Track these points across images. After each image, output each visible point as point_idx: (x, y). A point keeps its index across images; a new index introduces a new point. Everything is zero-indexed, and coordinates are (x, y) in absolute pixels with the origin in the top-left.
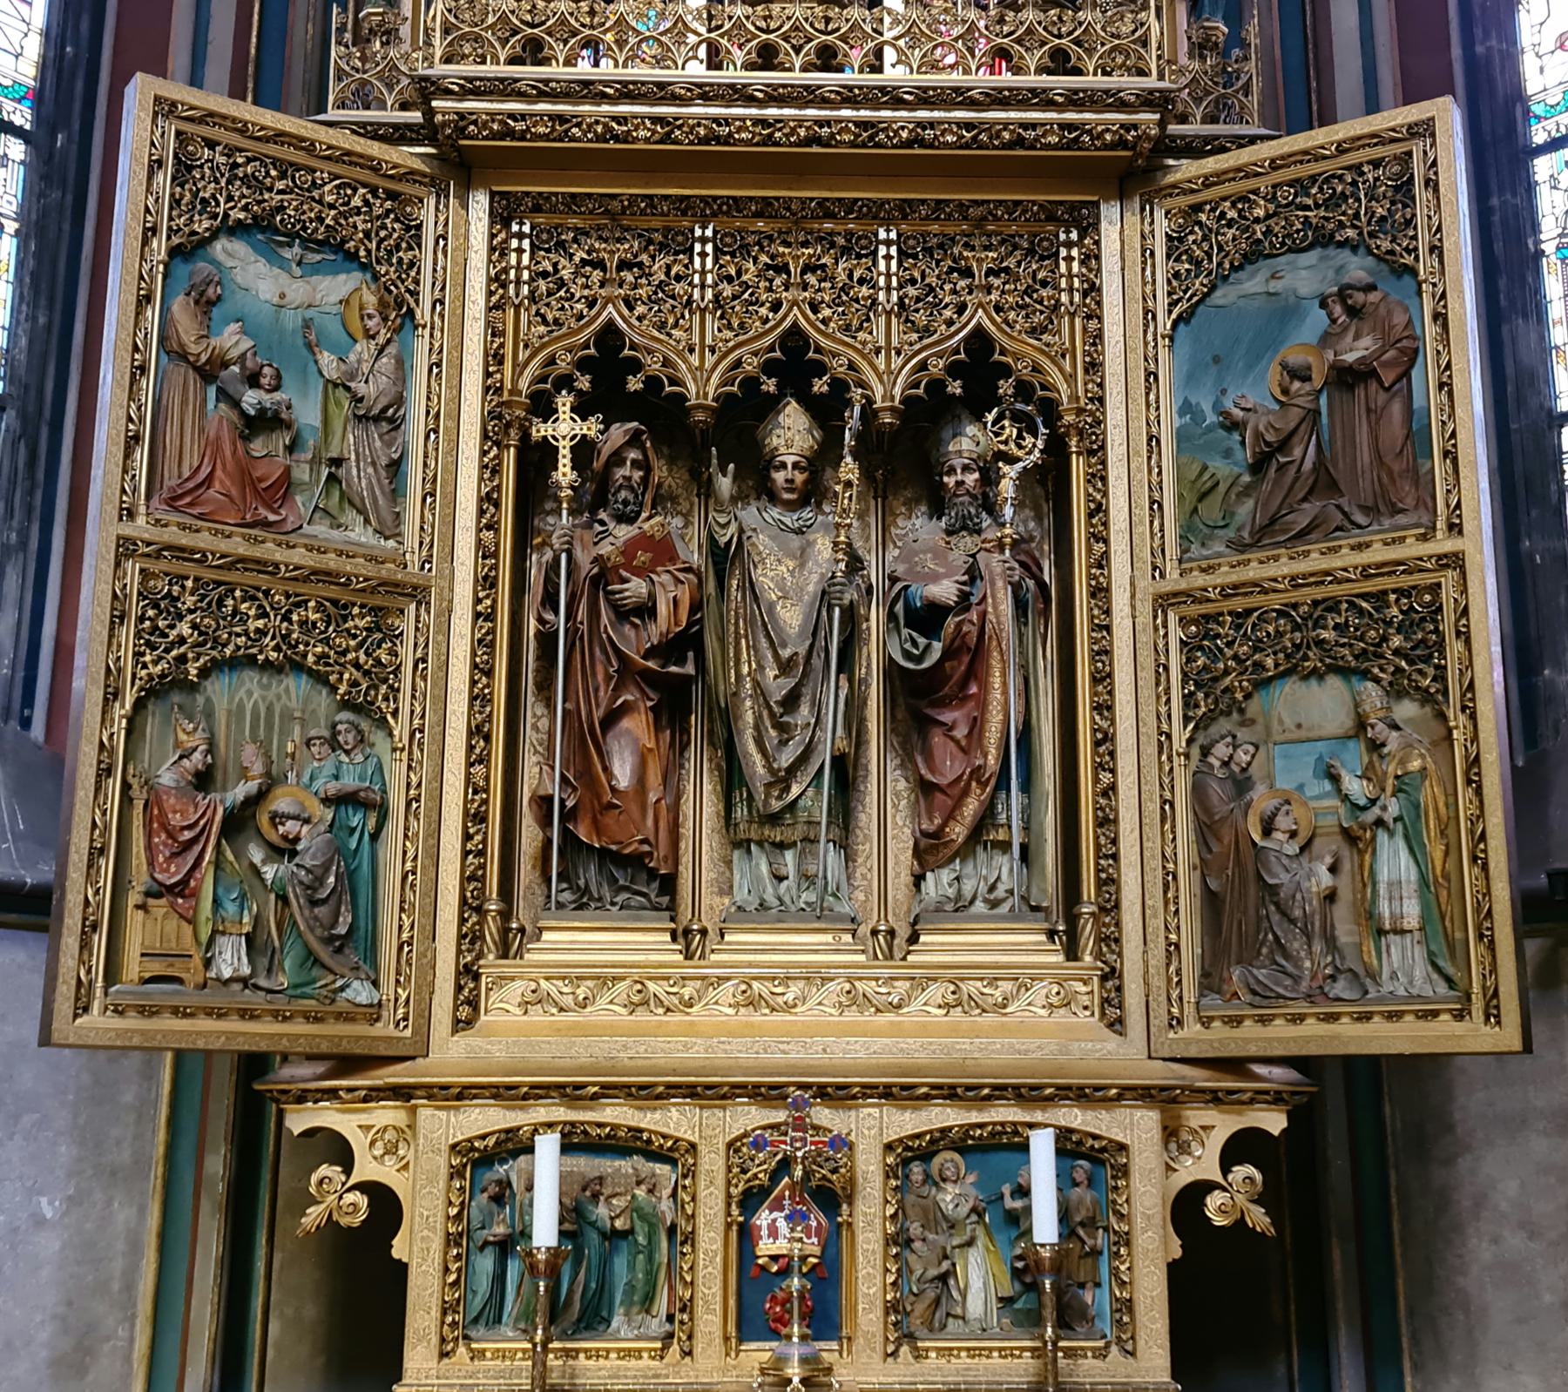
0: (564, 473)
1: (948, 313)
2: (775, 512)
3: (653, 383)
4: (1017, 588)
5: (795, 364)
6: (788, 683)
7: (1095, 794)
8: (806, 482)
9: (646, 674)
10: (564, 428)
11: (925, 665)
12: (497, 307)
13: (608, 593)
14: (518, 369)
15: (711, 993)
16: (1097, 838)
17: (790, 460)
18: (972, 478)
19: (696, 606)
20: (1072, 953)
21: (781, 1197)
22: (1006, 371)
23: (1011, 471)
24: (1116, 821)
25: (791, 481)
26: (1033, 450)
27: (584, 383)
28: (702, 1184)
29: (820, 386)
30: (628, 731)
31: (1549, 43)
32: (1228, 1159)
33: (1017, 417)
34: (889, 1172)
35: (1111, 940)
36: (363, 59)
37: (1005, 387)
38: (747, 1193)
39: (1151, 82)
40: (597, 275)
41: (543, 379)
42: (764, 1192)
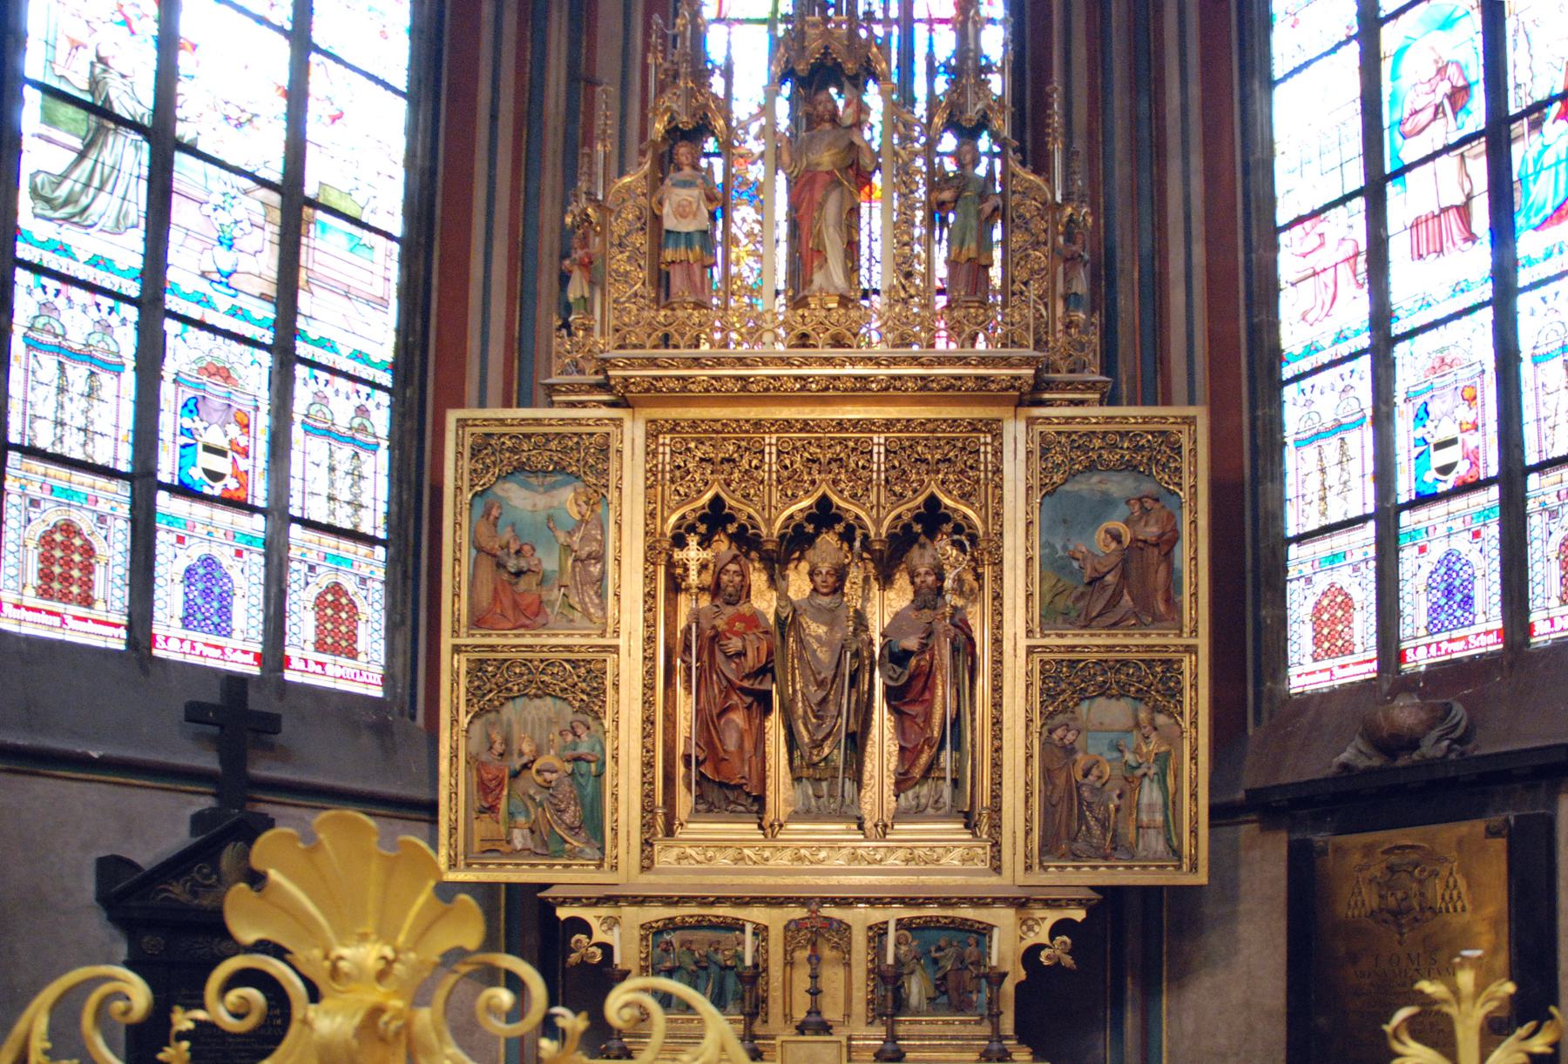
3: (742, 528)
6: (821, 694)
10: (692, 554)
14: (664, 520)
18: (930, 579)
19: (770, 653)
22: (947, 519)
27: (702, 528)
34: (870, 939)
35: (996, 826)
39: (1030, 352)
41: (679, 527)
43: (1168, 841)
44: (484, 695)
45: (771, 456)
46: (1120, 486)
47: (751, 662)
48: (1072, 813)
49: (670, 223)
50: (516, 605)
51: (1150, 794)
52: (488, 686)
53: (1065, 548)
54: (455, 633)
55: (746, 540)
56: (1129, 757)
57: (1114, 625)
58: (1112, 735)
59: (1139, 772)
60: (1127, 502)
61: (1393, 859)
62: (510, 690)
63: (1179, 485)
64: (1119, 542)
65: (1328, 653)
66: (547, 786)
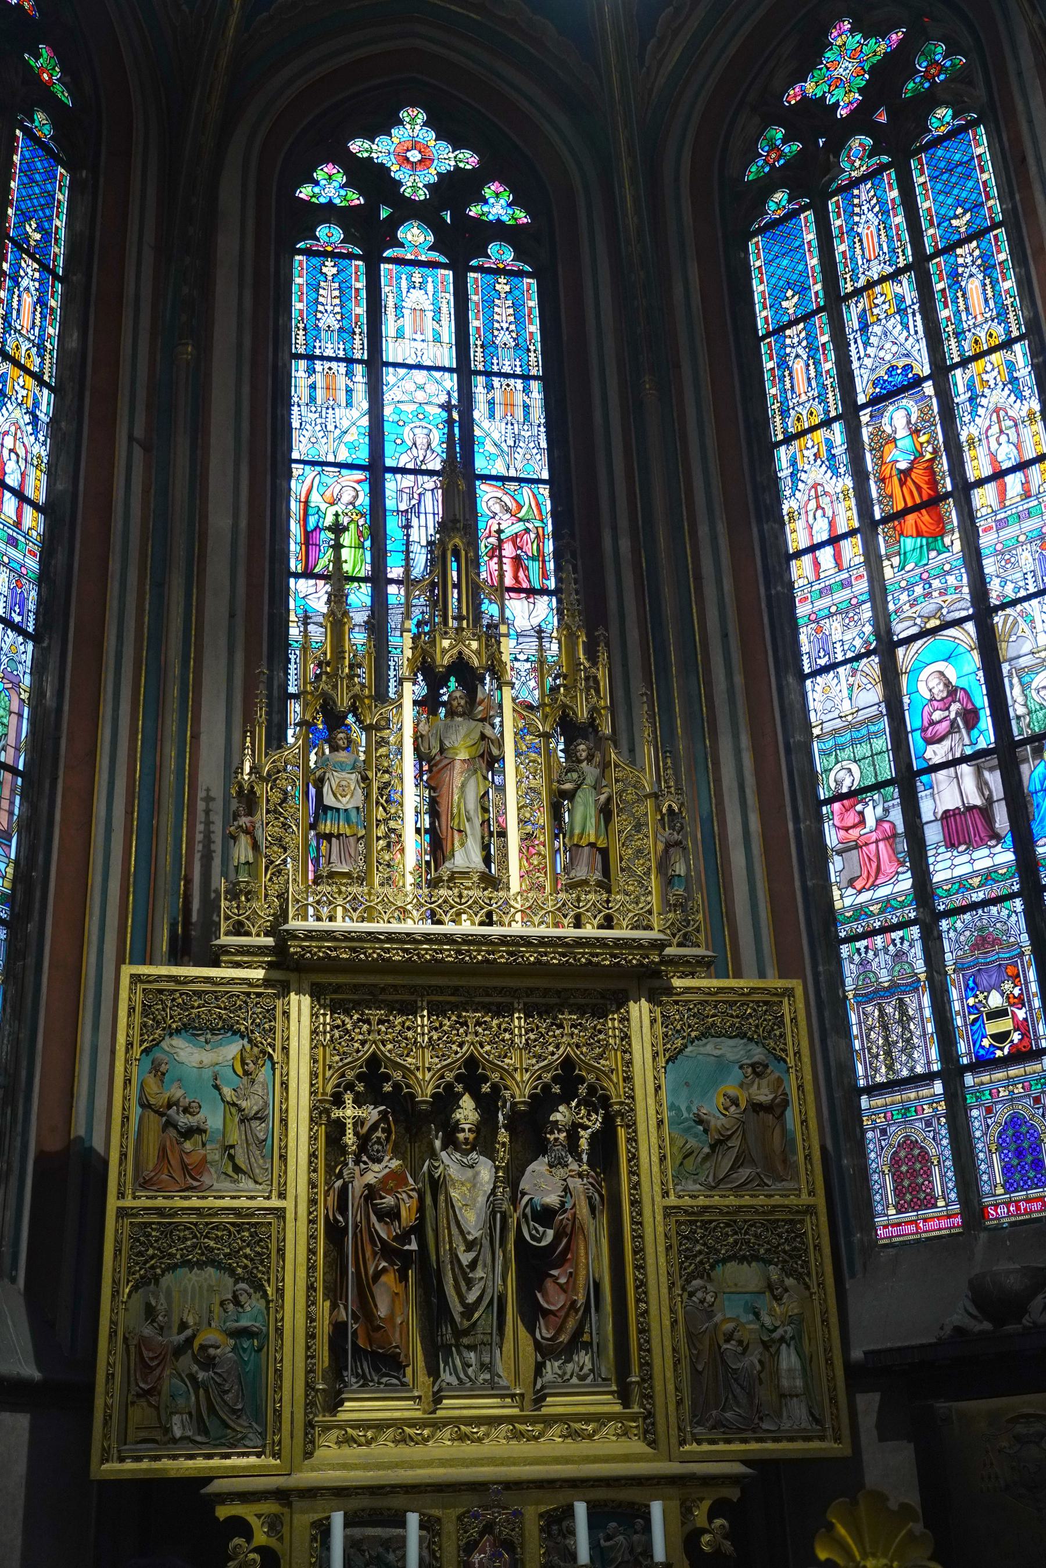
0: (350, 1138)
1: (551, 1048)
2: (458, 1155)
3: (397, 1086)
4: (590, 1198)
5: (472, 1074)
6: (471, 1255)
7: (637, 1316)
8: (475, 1139)
10: (349, 1112)
11: (543, 1244)
12: (316, 1047)
13: (374, 1205)
15: (439, 1434)
16: (639, 1339)
17: (467, 1127)
20: (626, 1405)
21: (485, 1545)
23: (585, 1134)
24: (649, 1331)
25: (466, 1139)
26: (596, 1121)
28: (444, 1540)
29: (486, 1088)
30: (385, 1284)
31: (844, 884)
32: (712, 1516)
34: (542, 1530)
36: (238, 908)
37: (582, 1090)
38: (467, 1544)
40: (365, 1027)
41: (338, 1086)
42: (476, 1543)
44: (146, 1262)
46: (731, 1049)
48: (721, 1387)
49: (329, 800)
50: (184, 1166)
52: (150, 1252)
54: (121, 1195)
56: (767, 1320)
58: (747, 1297)
59: (776, 1335)
60: (741, 1067)
61: (1020, 1429)
62: (172, 1256)
63: (784, 1050)
64: (737, 1105)
65: (915, 1205)
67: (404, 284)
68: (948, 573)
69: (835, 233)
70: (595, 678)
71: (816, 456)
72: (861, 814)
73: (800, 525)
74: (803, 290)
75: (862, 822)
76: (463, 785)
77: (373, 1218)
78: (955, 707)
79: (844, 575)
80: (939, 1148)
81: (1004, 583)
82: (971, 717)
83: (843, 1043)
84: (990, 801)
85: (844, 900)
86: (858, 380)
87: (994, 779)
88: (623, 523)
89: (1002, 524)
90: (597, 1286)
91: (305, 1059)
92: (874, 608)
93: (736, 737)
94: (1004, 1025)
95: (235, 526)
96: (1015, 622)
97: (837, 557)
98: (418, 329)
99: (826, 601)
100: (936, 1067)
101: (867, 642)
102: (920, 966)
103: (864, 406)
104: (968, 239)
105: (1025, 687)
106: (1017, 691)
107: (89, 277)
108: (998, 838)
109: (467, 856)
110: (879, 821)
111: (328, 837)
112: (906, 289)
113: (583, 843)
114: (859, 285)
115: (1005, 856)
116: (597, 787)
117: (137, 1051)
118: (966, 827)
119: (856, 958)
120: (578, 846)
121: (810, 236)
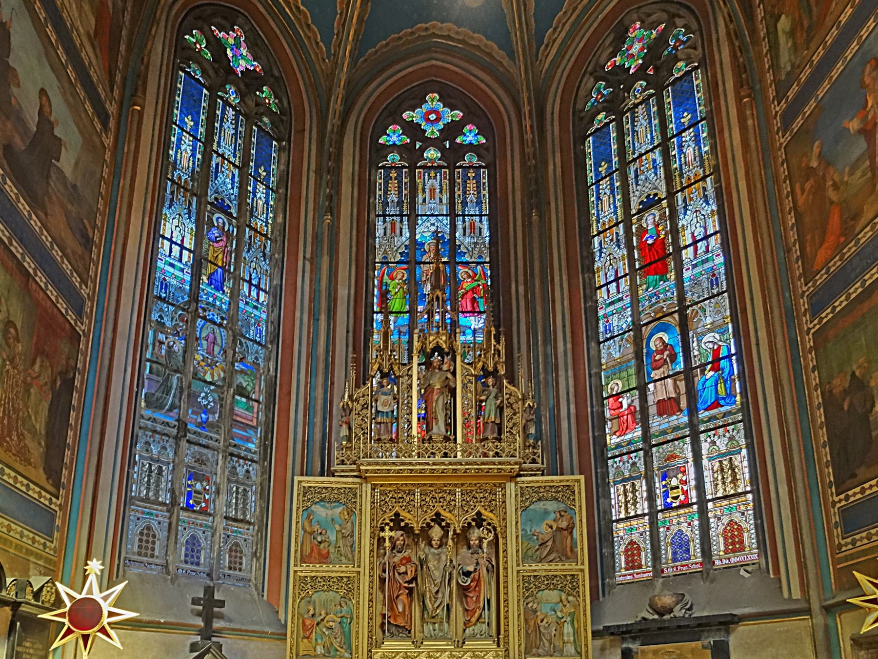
3: (407, 524)
5: (438, 518)
9: (406, 588)
10: (387, 534)
14: (377, 522)
26: (491, 537)
27: (392, 524)
29: (443, 524)
33: (487, 529)
37: (485, 523)
43: (576, 649)
45: (418, 496)
46: (551, 506)
47: (409, 577)
51: (568, 629)
53: (531, 531)
54: (296, 565)
55: (408, 530)
57: (551, 561)
59: (563, 620)
66: (330, 628)
67: (426, 177)
68: (668, 291)
69: (626, 131)
70: (499, 351)
71: (612, 240)
72: (621, 403)
73: (602, 273)
74: (610, 161)
75: (621, 407)
76: (438, 399)
77: (396, 574)
78: (666, 353)
79: (620, 296)
80: (646, 545)
81: (693, 295)
82: (673, 357)
83: (606, 502)
84: (679, 394)
85: (612, 440)
86: (632, 203)
87: (682, 385)
88: (521, 278)
89: (695, 266)
90: (489, 601)
91: (368, 514)
92: (632, 310)
93: (566, 371)
94: (679, 492)
95: (349, 293)
96: (697, 312)
97: (618, 287)
98: (433, 197)
99: (611, 308)
100: (646, 511)
101: (629, 326)
102: (642, 469)
103: (634, 215)
104: (689, 128)
105: (699, 342)
106: (695, 344)
107: (287, 190)
108: (681, 411)
109: (439, 428)
110: (629, 406)
111: (380, 423)
112: (657, 155)
113: (489, 421)
114: (635, 156)
115: (685, 419)
116: (496, 398)
117: (301, 510)
118: (667, 407)
119: (615, 465)
120: (487, 423)
121: (613, 135)
